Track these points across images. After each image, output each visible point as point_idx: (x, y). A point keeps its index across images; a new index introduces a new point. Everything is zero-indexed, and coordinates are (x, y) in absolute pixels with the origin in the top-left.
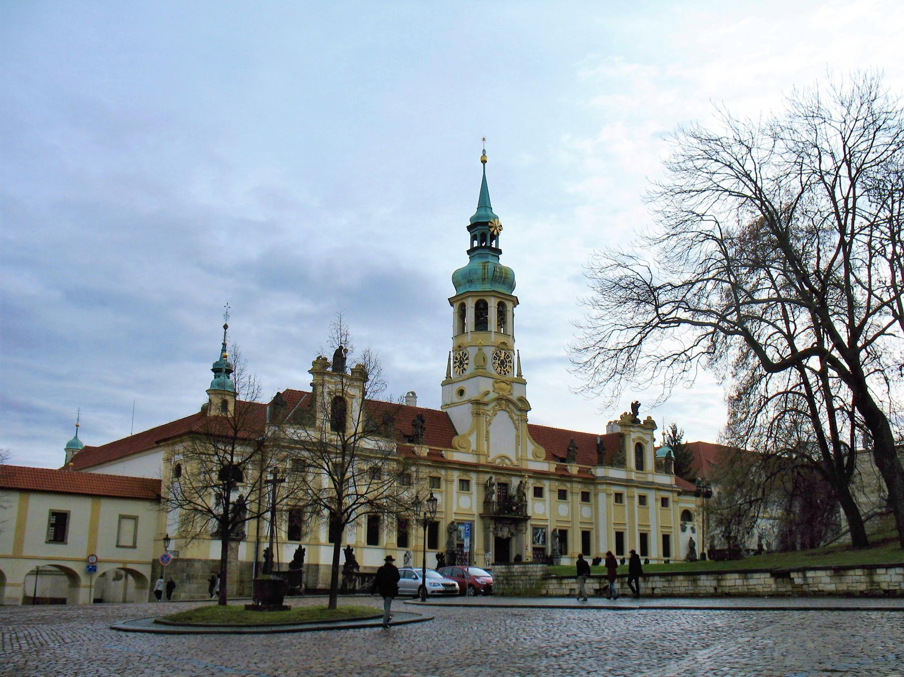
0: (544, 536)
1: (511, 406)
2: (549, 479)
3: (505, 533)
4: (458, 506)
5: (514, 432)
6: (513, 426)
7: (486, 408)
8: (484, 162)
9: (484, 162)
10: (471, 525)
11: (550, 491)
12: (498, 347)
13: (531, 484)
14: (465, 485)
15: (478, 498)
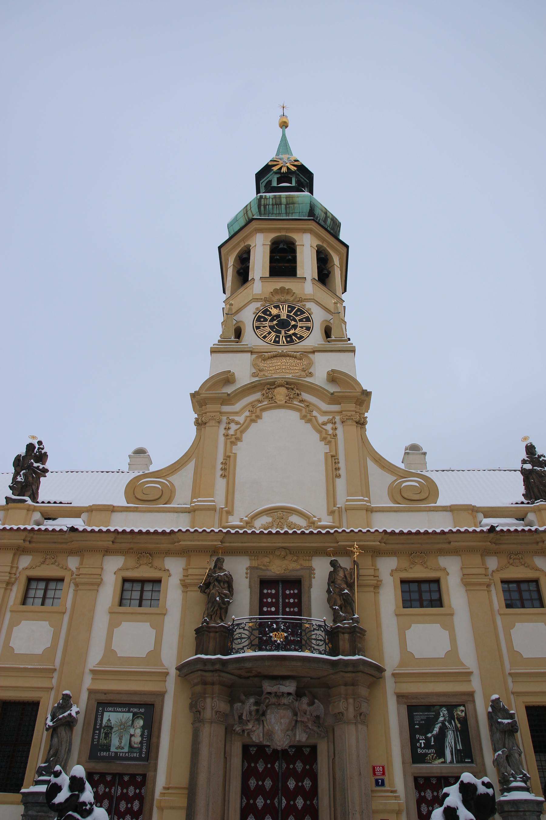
0: (465, 731)
1: (305, 396)
2: (455, 552)
3: (278, 729)
4: (109, 653)
5: (322, 449)
6: (317, 436)
7: (226, 408)
8: (284, 125)
9: (284, 125)
10: (147, 710)
11: (468, 583)
12: (266, 300)
13: (388, 569)
14: (139, 592)
15: (182, 624)
